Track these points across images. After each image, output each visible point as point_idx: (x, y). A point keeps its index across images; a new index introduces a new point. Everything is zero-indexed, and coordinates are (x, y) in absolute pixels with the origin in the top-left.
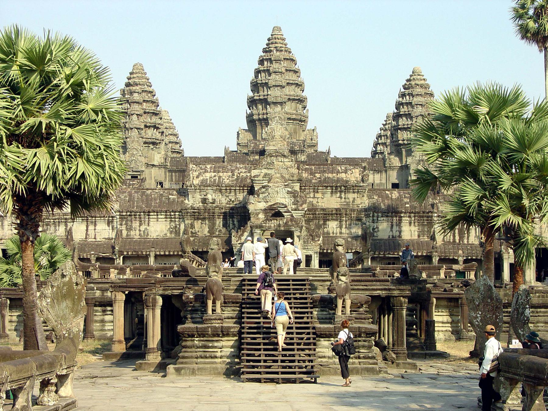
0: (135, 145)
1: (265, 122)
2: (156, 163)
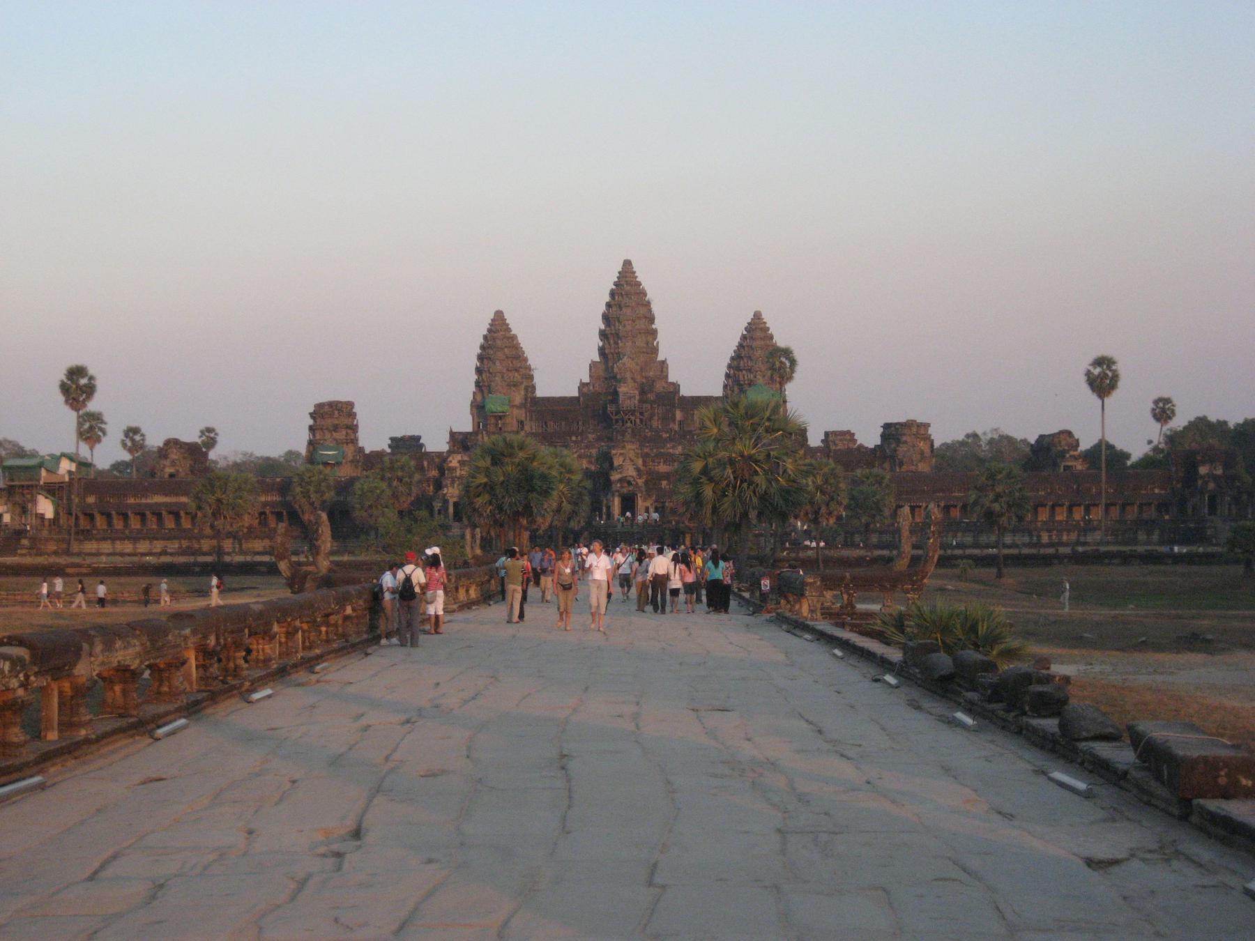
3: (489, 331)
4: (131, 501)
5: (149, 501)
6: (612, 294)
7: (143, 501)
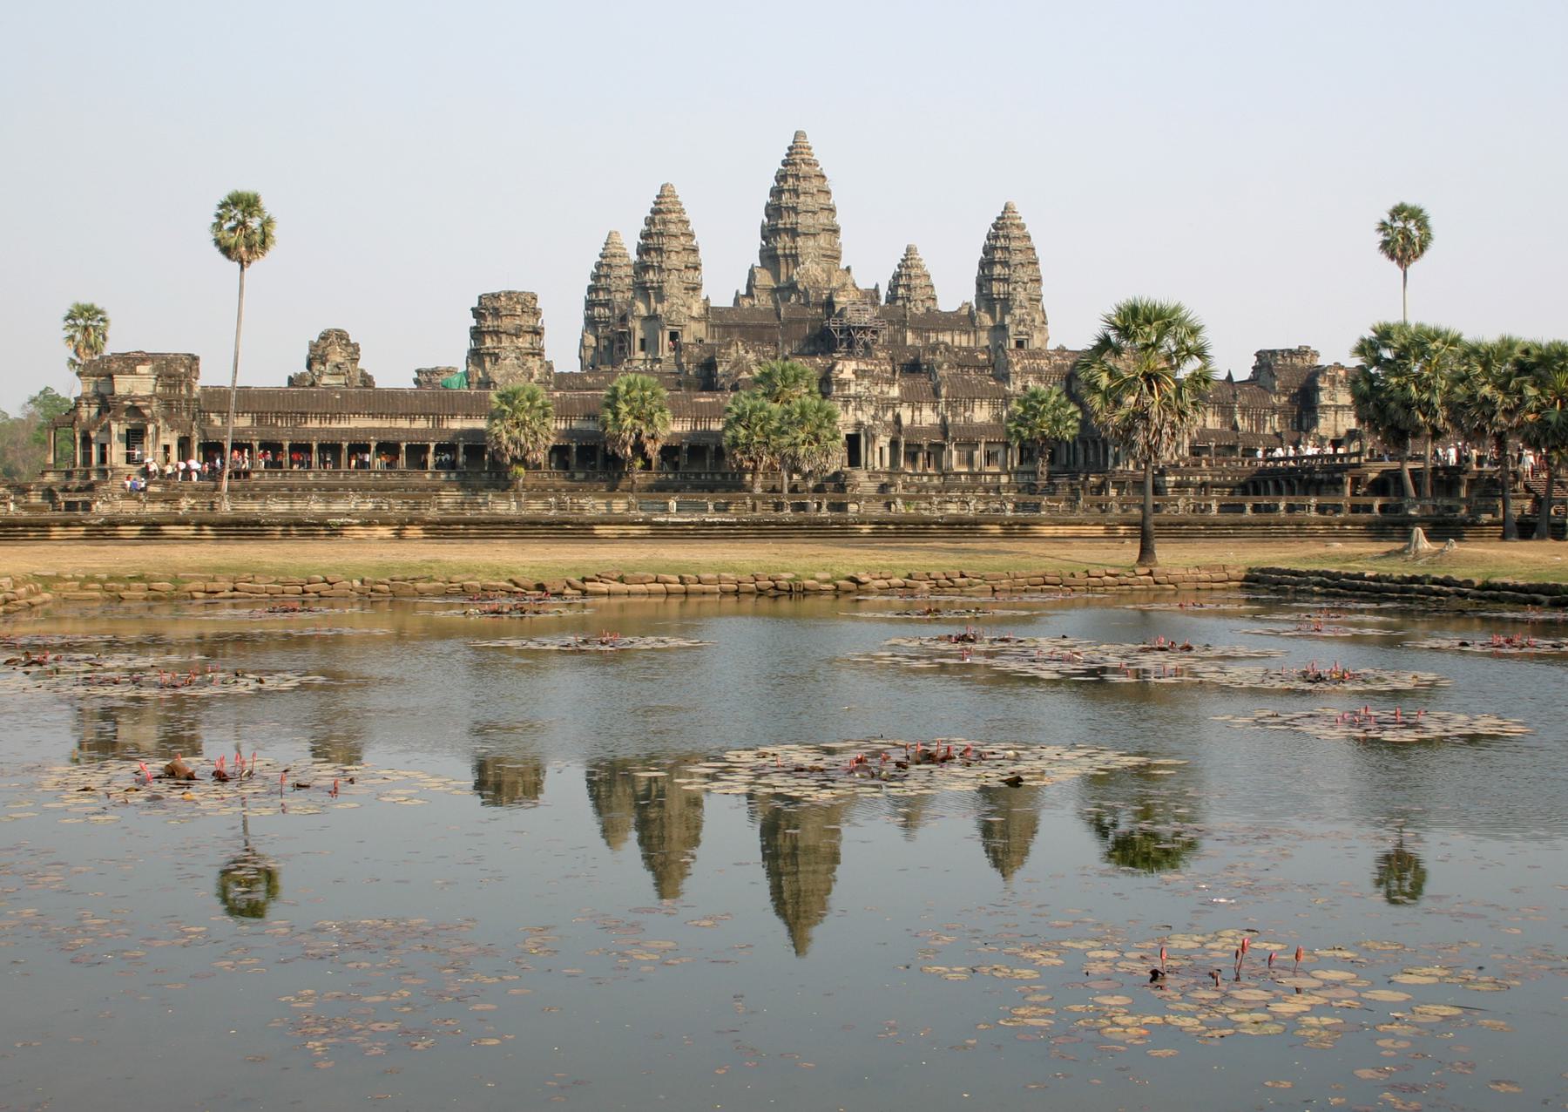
0: (675, 291)
1: (794, 259)
2: (694, 314)
3: (654, 212)
4: (314, 424)
5: (343, 425)
6: (781, 177)
7: (335, 425)
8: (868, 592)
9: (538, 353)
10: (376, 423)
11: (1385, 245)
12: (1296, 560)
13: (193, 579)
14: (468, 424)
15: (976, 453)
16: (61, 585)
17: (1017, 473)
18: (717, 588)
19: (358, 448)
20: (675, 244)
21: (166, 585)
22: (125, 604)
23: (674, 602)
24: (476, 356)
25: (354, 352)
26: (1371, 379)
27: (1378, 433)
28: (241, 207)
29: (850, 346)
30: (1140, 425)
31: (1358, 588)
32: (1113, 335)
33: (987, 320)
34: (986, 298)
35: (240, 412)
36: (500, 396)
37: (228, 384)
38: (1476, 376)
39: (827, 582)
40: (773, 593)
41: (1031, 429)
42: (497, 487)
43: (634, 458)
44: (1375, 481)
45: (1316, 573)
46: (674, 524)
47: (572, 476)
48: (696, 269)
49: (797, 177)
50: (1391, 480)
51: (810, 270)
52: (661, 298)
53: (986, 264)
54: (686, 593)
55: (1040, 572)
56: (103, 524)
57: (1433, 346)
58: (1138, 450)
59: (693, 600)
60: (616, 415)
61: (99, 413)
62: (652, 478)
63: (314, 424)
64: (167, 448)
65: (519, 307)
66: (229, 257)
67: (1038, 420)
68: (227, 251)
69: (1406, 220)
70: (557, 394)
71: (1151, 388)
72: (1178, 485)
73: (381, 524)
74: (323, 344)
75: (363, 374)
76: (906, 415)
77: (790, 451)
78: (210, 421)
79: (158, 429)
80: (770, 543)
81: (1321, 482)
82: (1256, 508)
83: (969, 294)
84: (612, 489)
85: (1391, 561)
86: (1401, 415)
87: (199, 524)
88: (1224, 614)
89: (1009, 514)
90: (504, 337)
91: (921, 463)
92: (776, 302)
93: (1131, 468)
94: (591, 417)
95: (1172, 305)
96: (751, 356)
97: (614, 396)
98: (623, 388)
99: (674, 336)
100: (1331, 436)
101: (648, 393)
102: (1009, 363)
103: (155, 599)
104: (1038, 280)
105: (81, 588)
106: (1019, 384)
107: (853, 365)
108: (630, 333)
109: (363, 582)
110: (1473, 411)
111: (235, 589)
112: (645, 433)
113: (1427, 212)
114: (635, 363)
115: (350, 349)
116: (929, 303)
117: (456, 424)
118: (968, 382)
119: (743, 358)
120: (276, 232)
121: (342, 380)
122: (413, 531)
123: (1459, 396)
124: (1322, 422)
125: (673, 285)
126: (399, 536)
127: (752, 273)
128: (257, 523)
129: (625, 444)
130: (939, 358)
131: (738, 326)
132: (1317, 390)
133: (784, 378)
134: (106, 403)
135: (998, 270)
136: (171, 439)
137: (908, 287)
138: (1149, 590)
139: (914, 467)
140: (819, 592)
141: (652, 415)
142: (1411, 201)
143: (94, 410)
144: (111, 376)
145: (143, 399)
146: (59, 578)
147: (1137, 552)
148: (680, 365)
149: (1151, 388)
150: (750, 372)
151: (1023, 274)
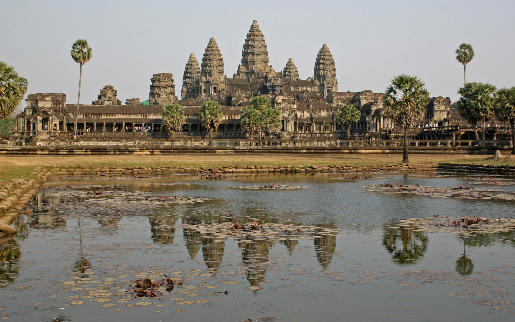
0: (215, 73)
1: (253, 63)
2: (222, 81)
4: (104, 117)
5: (114, 117)
6: (249, 36)
7: (111, 117)
8: (316, 172)
9: (173, 94)
10: (125, 117)
11: (458, 57)
12: (453, 161)
13: (96, 167)
14: (155, 117)
15: (322, 126)
16: (53, 170)
17: (335, 133)
18: (267, 170)
19: (119, 126)
20: (215, 58)
21: (88, 170)
22: (74, 176)
23: (254, 175)
24: (152, 94)
25: (115, 93)
26: (465, 102)
27: (467, 119)
28: (81, 45)
29: (273, 91)
30: (404, 116)
31: (481, 170)
32: (394, 86)
33: (318, 83)
34: (317, 75)
35: (80, 113)
36: (167, 108)
37: (75, 103)
38: (504, 100)
39: (303, 168)
40: (285, 172)
41: (344, 118)
42: (165, 138)
43: (210, 128)
44: (463, 135)
45: (465, 165)
46: (242, 149)
47: (189, 134)
48: (222, 66)
49: (254, 35)
50: (469, 135)
51: (259, 66)
52: (211, 76)
53: (317, 64)
54: (257, 172)
55: (372, 165)
56: (54, 150)
57: (486, 90)
58: (403, 125)
59: (259, 174)
60: (205, 114)
61: (33, 113)
62: (216, 135)
63: (104, 117)
64: (55, 125)
65: (167, 78)
66: (77, 61)
67: (347, 115)
68: (76, 59)
69: (465, 49)
70: (184, 107)
71: (407, 104)
72: (395, 137)
73: (146, 150)
74: (105, 90)
75: (118, 100)
76: (299, 114)
77: (265, 126)
78: (70, 116)
79: (53, 118)
80: (274, 156)
81: (445, 135)
82: (430, 144)
83: (312, 75)
84: (203, 138)
85: (489, 161)
86: (475, 113)
87: (86, 150)
88: (427, 178)
89: (350, 146)
90: (162, 88)
91: (304, 130)
92: (247, 76)
93: (374, 131)
94: (197, 115)
95: (414, 77)
96: (243, 95)
97: (204, 108)
98: (207, 105)
99: (215, 88)
100: (439, 120)
101: (215, 107)
102: (332, 97)
103: (84, 174)
104: (335, 69)
105: (60, 170)
106: (336, 104)
107: (282, 97)
108: (200, 87)
109: (152, 168)
110: (503, 112)
111: (110, 171)
112: (214, 120)
113: (472, 46)
114: (202, 97)
115: (114, 92)
116: (296, 77)
117: (151, 117)
118: (319, 103)
119: (240, 96)
120: (92, 53)
121: (111, 102)
122: (157, 152)
123: (498, 107)
124: (435, 116)
125: (215, 71)
126: (152, 154)
127: (239, 67)
128: (105, 149)
129: (208, 124)
130: (305, 95)
131: (235, 85)
132: (434, 105)
133: (260, 101)
134: (35, 110)
135: (321, 66)
136: (57, 122)
137: (289, 72)
138: (407, 171)
139: (301, 131)
140: (301, 172)
141: (216, 114)
142: (467, 43)
143: (31, 112)
144: (37, 101)
145: (48, 108)
146: (52, 167)
147: (402, 159)
148: (219, 98)
149: (407, 104)
150: (243, 100)
151: (330, 68)
